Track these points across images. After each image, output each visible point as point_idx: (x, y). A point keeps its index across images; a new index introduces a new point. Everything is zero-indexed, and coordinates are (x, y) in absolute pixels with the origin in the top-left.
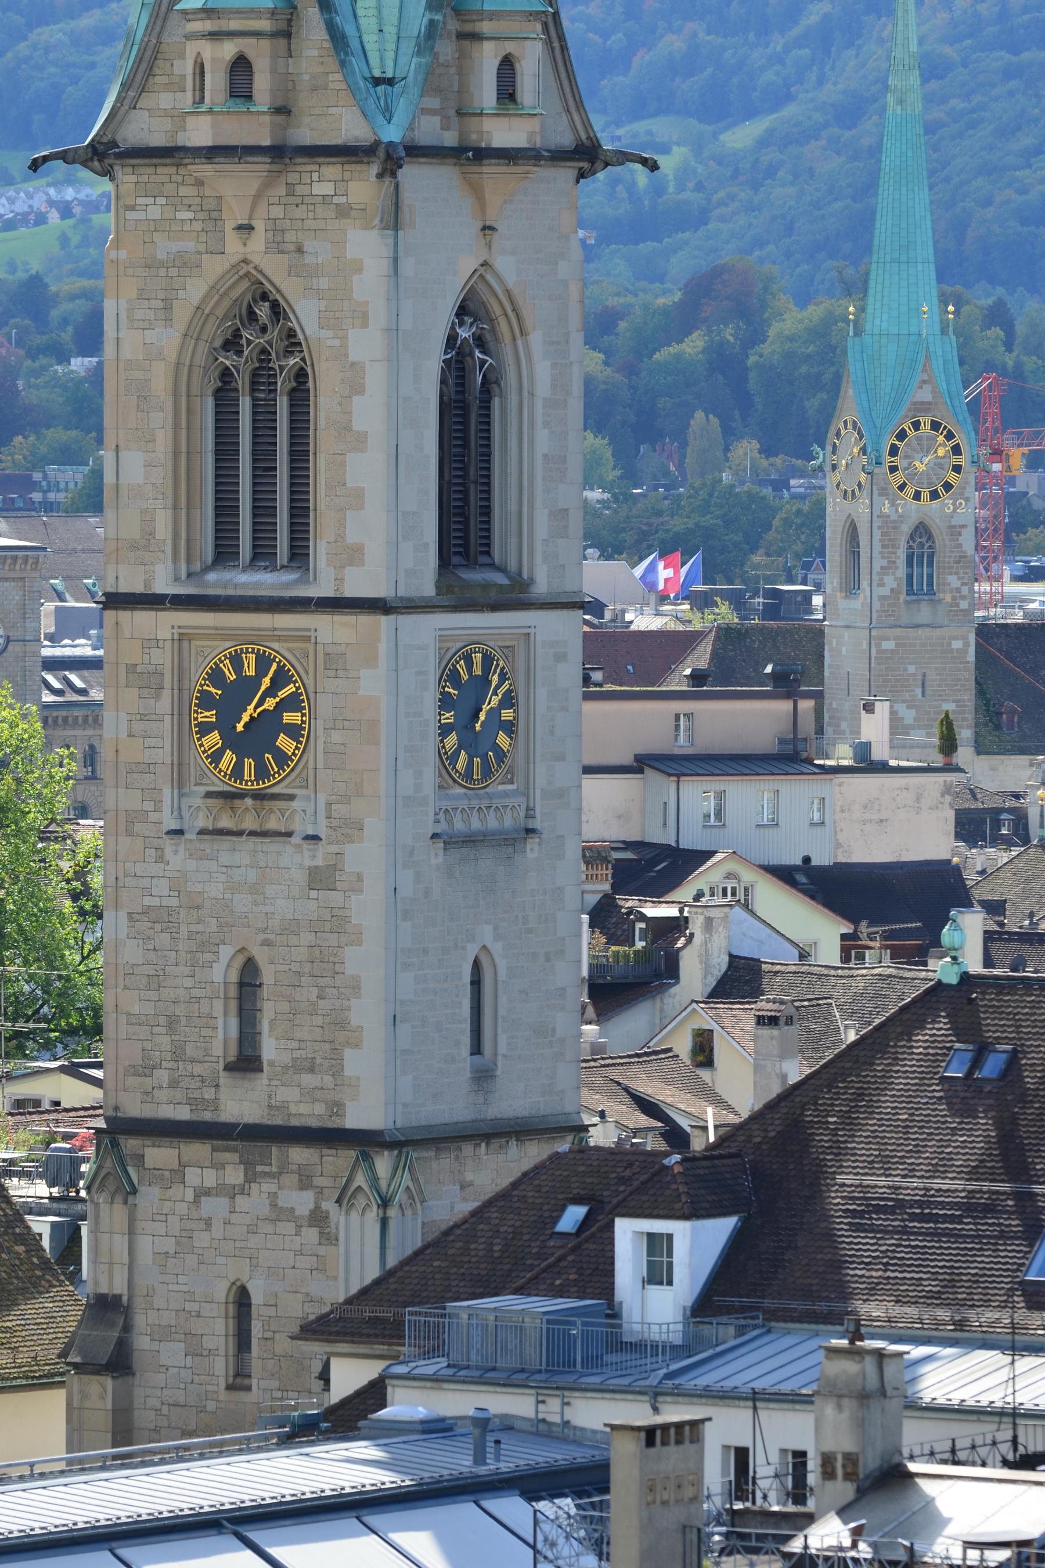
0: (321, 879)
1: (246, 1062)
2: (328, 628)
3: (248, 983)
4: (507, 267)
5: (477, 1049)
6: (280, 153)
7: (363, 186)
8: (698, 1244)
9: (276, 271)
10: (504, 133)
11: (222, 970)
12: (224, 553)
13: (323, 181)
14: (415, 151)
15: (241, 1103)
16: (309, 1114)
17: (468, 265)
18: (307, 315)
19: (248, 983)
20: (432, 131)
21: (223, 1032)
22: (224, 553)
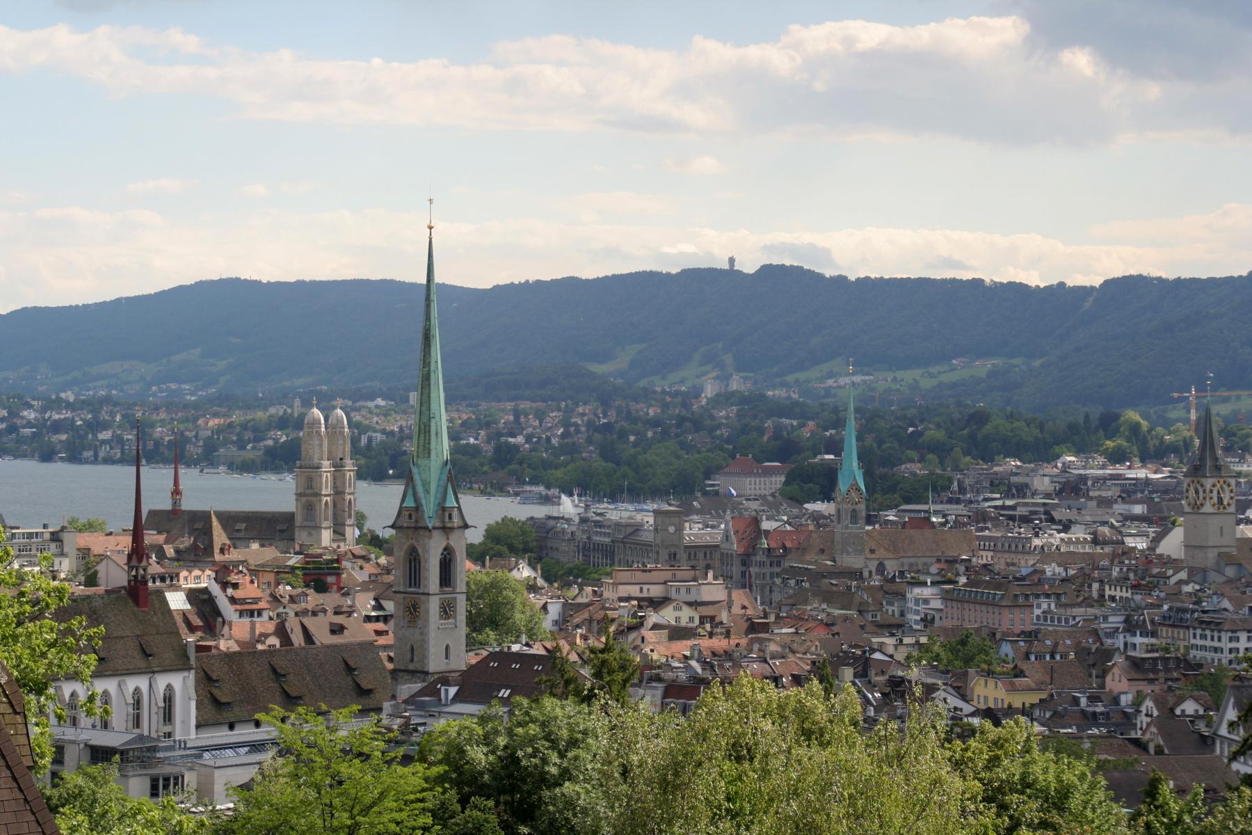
0: (422, 634)
1: (412, 660)
2: (423, 597)
3: (412, 649)
4: (452, 543)
5: (447, 657)
6: (416, 528)
7: (427, 533)
8: (453, 691)
9: (416, 544)
10: (449, 525)
11: (408, 647)
12: (410, 585)
13: (422, 532)
14: (434, 528)
15: (411, 667)
16: (420, 668)
17: (444, 545)
18: (420, 550)
19: (412, 649)
20: (438, 524)
21: (409, 656)
22: (410, 585)
